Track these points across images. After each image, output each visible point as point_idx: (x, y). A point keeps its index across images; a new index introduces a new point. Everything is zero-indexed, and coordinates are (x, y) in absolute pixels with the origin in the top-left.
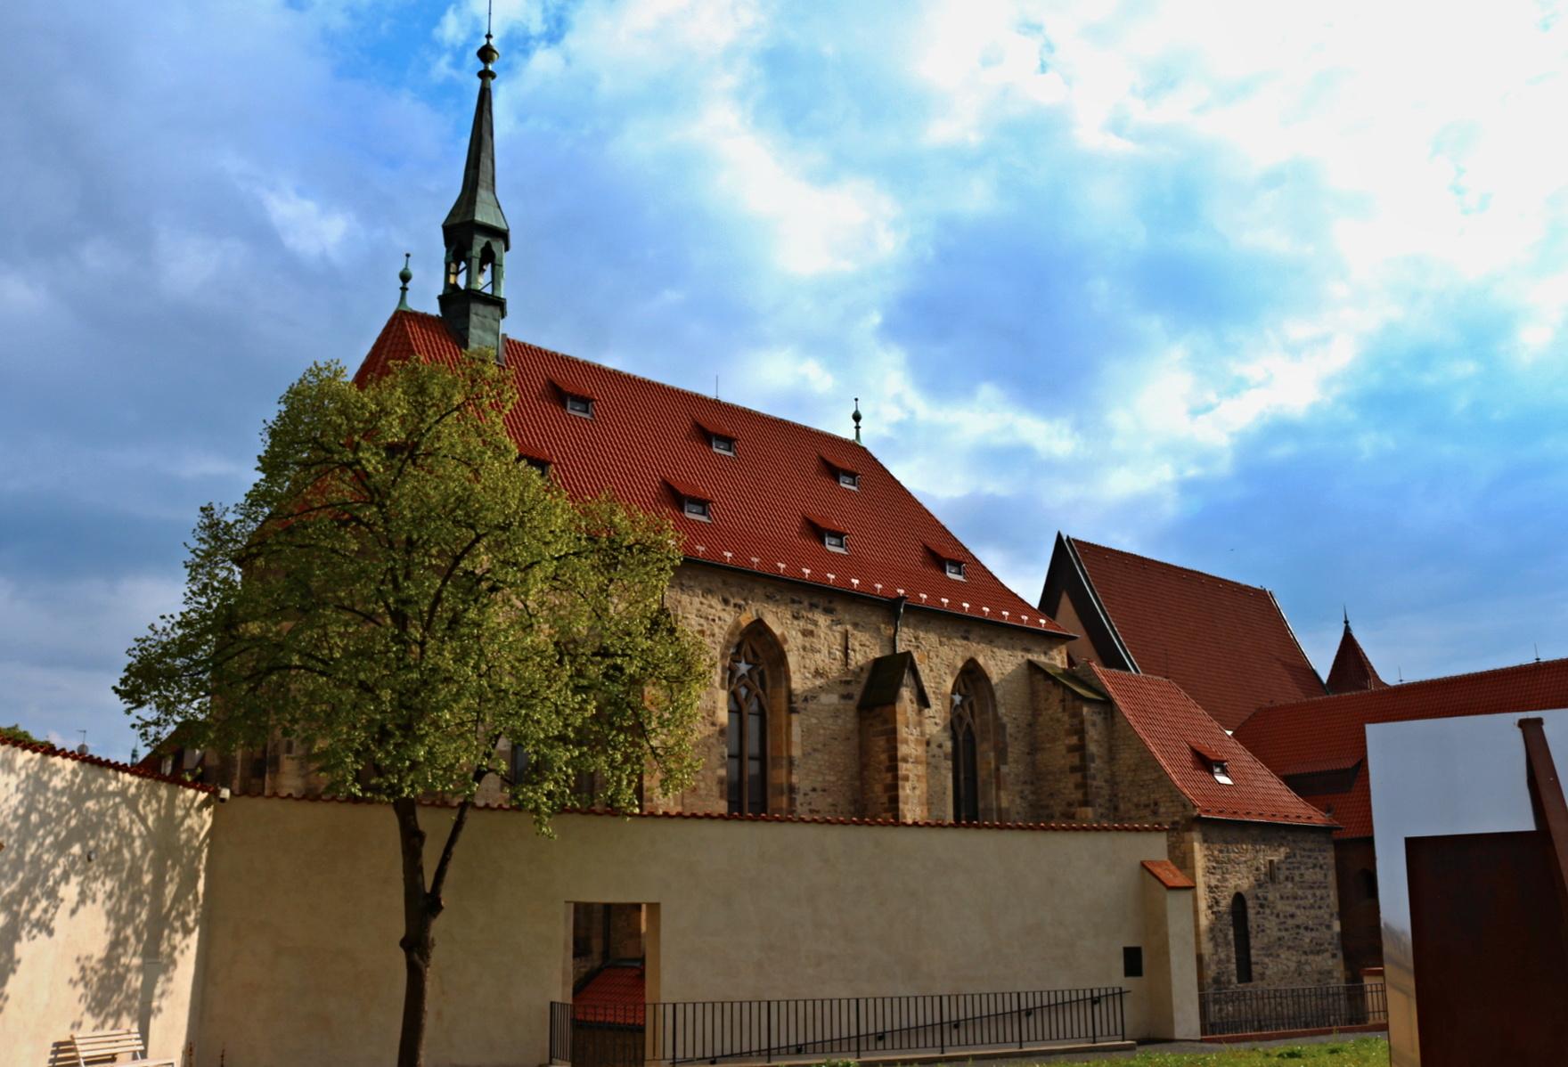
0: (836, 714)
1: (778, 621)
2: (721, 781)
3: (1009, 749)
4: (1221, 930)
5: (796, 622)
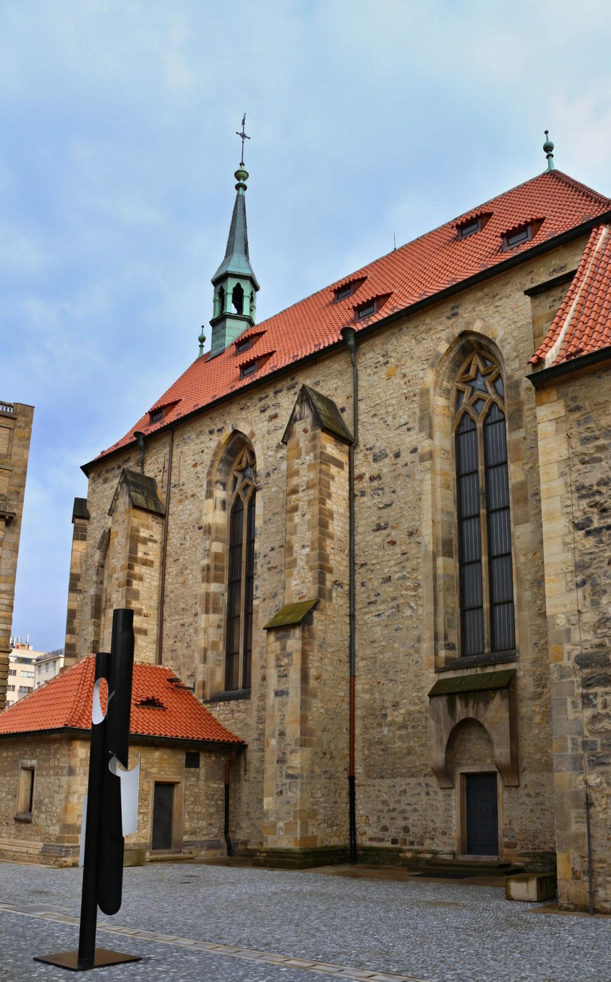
5: (262, 416)
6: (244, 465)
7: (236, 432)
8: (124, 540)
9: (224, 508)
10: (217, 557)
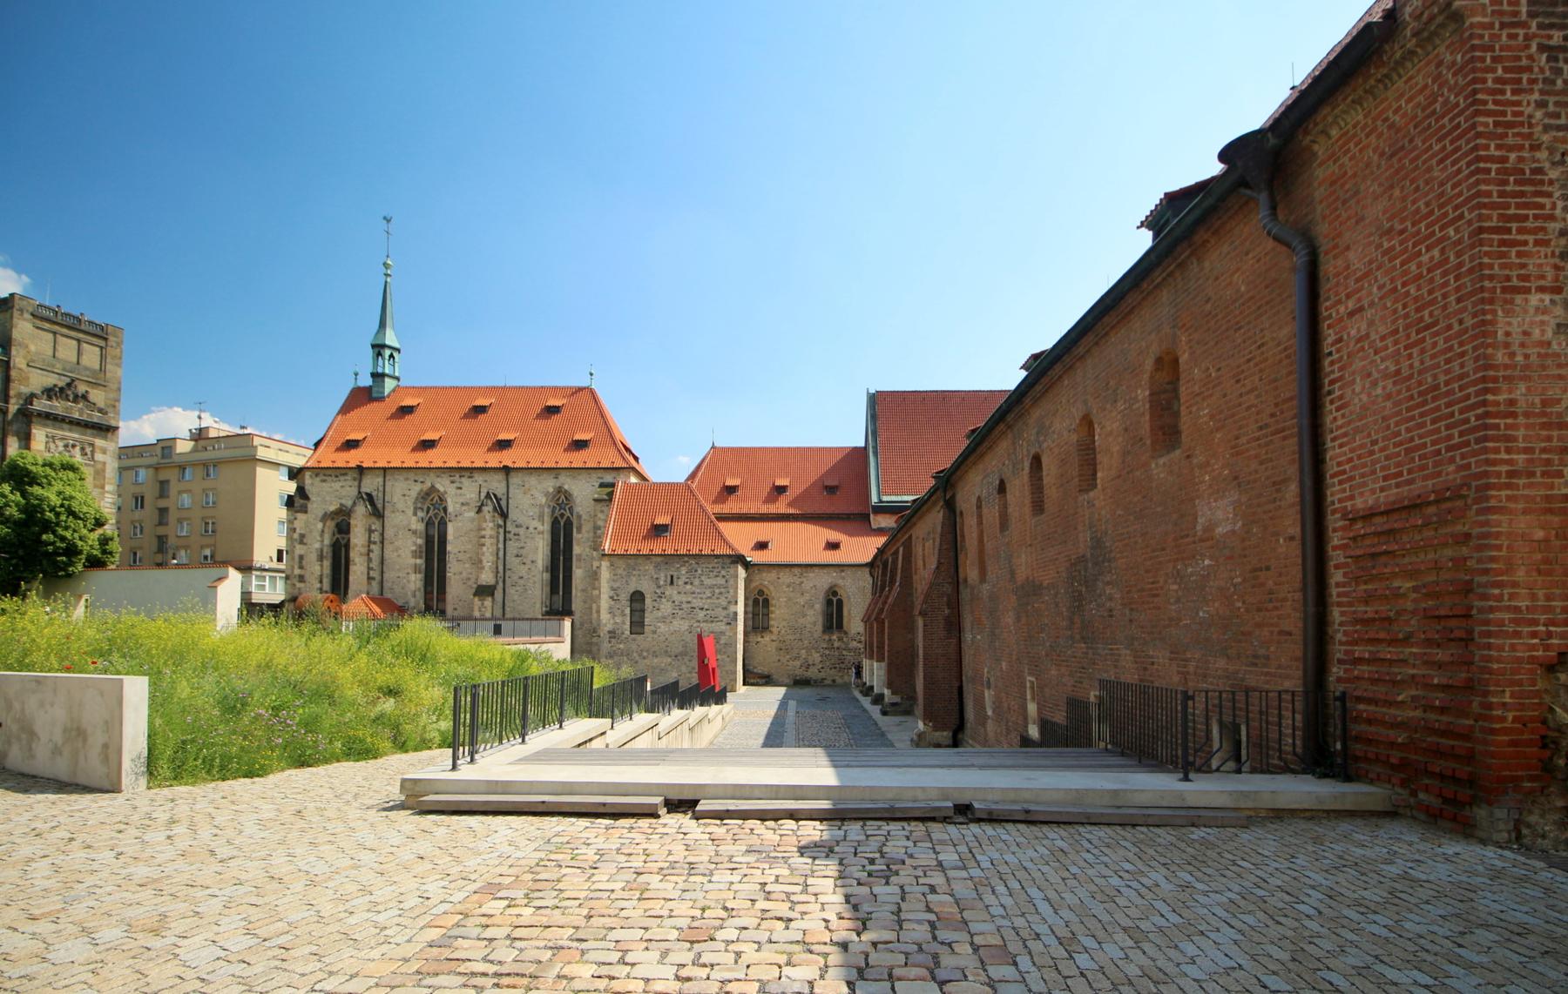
0: (472, 520)
1: (443, 484)
2: (412, 552)
7: (433, 486)
10: (420, 546)
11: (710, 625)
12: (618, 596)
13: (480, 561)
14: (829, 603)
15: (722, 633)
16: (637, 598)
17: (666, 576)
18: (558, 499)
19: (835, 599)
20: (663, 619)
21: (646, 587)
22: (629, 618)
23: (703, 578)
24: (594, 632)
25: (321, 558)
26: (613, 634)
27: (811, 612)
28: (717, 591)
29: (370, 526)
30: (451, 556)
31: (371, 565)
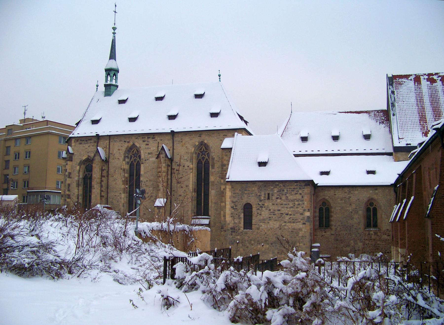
3: (215, 165)
4: (237, 214)
5: (144, 143)
6: (134, 153)
7: (134, 144)
8: (99, 170)
9: (128, 164)
10: (127, 178)
11: (292, 224)
12: (236, 206)
13: (158, 186)
14: (368, 210)
15: (300, 229)
16: (248, 208)
17: (265, 194)
18: (201, 149)
19: (372, 208)
20: (263, 221)
21: (253, 201)
22: (243, 220)
23: (288, 195)
24: (222, 228)
25: (78, 185)
26: (233, 229)
27: (356, 216)
28: (297, 203)
29: (102, 167)
30: (143, 183)
31: (102, 189)
